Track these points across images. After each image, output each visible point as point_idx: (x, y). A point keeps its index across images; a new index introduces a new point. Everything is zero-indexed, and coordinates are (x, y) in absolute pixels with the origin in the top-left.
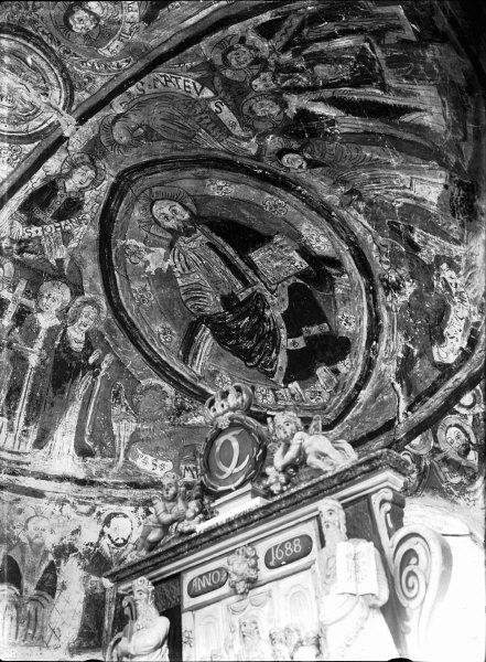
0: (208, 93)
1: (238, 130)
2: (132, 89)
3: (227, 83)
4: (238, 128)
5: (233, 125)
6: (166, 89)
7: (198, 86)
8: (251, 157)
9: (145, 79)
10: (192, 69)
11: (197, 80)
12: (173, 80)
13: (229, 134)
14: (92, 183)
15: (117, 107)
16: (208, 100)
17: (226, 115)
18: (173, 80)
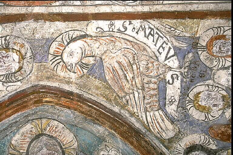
0: (174, 63)
1: (171, 109)
2: (118, 24)
3: (195, 63)
4: (174, 107)
5: (171, 103)
6: (145, 40)
7: (172, 52)
8: (162, 141)
9: (134, 22)
10: (177, 38)
11: (175, 48)
12: (156, 36)
13: (162, 107)
14: (7, 76)
15: (92, 27)
16: (170, 68)
17: (173, 91)
18: (156, 36)
